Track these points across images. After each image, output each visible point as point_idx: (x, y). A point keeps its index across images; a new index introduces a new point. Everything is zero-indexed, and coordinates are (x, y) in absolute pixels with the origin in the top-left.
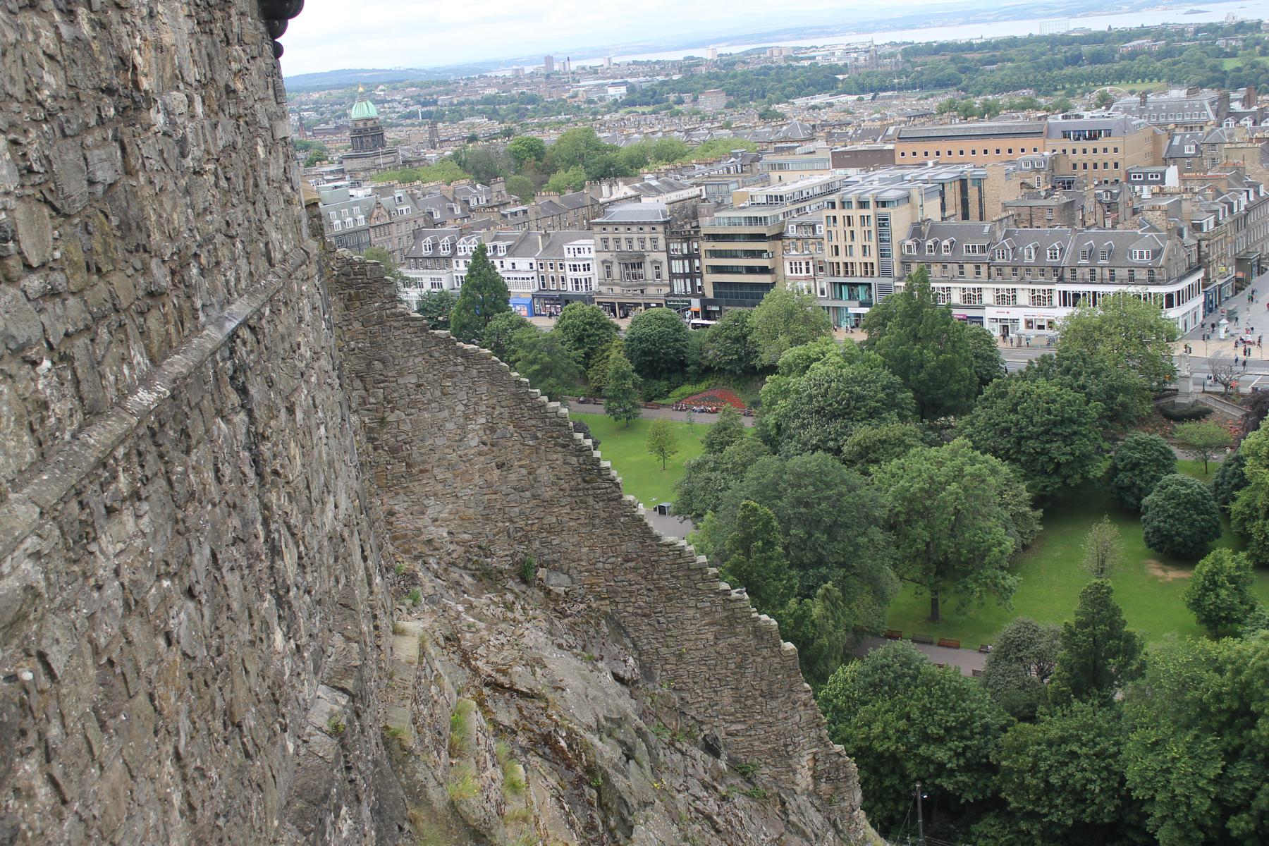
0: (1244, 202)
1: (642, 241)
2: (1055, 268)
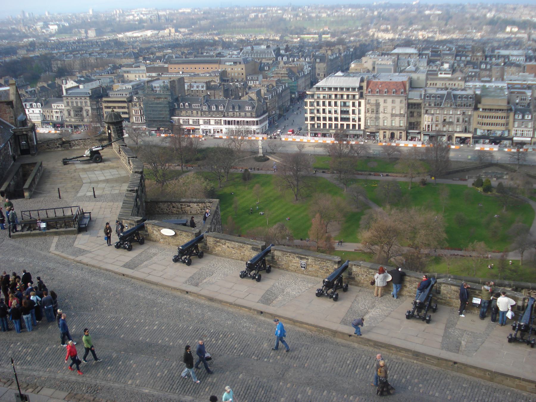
0: (281, 89)
1: (81, 103)
2: (222, 112)
